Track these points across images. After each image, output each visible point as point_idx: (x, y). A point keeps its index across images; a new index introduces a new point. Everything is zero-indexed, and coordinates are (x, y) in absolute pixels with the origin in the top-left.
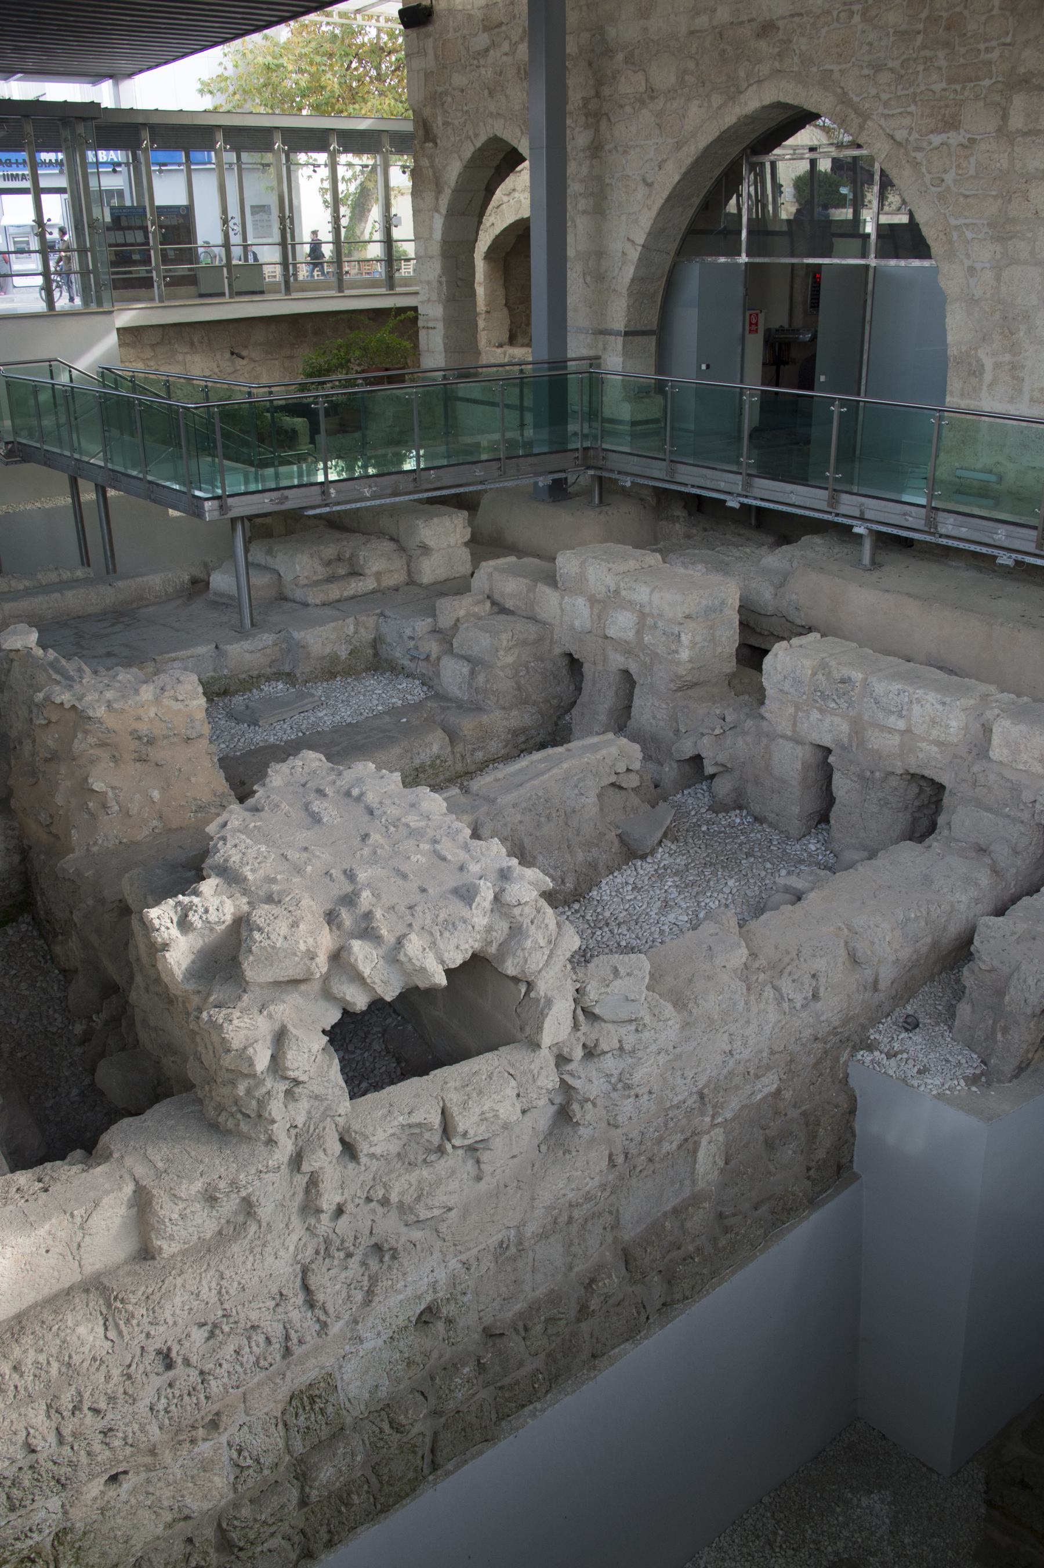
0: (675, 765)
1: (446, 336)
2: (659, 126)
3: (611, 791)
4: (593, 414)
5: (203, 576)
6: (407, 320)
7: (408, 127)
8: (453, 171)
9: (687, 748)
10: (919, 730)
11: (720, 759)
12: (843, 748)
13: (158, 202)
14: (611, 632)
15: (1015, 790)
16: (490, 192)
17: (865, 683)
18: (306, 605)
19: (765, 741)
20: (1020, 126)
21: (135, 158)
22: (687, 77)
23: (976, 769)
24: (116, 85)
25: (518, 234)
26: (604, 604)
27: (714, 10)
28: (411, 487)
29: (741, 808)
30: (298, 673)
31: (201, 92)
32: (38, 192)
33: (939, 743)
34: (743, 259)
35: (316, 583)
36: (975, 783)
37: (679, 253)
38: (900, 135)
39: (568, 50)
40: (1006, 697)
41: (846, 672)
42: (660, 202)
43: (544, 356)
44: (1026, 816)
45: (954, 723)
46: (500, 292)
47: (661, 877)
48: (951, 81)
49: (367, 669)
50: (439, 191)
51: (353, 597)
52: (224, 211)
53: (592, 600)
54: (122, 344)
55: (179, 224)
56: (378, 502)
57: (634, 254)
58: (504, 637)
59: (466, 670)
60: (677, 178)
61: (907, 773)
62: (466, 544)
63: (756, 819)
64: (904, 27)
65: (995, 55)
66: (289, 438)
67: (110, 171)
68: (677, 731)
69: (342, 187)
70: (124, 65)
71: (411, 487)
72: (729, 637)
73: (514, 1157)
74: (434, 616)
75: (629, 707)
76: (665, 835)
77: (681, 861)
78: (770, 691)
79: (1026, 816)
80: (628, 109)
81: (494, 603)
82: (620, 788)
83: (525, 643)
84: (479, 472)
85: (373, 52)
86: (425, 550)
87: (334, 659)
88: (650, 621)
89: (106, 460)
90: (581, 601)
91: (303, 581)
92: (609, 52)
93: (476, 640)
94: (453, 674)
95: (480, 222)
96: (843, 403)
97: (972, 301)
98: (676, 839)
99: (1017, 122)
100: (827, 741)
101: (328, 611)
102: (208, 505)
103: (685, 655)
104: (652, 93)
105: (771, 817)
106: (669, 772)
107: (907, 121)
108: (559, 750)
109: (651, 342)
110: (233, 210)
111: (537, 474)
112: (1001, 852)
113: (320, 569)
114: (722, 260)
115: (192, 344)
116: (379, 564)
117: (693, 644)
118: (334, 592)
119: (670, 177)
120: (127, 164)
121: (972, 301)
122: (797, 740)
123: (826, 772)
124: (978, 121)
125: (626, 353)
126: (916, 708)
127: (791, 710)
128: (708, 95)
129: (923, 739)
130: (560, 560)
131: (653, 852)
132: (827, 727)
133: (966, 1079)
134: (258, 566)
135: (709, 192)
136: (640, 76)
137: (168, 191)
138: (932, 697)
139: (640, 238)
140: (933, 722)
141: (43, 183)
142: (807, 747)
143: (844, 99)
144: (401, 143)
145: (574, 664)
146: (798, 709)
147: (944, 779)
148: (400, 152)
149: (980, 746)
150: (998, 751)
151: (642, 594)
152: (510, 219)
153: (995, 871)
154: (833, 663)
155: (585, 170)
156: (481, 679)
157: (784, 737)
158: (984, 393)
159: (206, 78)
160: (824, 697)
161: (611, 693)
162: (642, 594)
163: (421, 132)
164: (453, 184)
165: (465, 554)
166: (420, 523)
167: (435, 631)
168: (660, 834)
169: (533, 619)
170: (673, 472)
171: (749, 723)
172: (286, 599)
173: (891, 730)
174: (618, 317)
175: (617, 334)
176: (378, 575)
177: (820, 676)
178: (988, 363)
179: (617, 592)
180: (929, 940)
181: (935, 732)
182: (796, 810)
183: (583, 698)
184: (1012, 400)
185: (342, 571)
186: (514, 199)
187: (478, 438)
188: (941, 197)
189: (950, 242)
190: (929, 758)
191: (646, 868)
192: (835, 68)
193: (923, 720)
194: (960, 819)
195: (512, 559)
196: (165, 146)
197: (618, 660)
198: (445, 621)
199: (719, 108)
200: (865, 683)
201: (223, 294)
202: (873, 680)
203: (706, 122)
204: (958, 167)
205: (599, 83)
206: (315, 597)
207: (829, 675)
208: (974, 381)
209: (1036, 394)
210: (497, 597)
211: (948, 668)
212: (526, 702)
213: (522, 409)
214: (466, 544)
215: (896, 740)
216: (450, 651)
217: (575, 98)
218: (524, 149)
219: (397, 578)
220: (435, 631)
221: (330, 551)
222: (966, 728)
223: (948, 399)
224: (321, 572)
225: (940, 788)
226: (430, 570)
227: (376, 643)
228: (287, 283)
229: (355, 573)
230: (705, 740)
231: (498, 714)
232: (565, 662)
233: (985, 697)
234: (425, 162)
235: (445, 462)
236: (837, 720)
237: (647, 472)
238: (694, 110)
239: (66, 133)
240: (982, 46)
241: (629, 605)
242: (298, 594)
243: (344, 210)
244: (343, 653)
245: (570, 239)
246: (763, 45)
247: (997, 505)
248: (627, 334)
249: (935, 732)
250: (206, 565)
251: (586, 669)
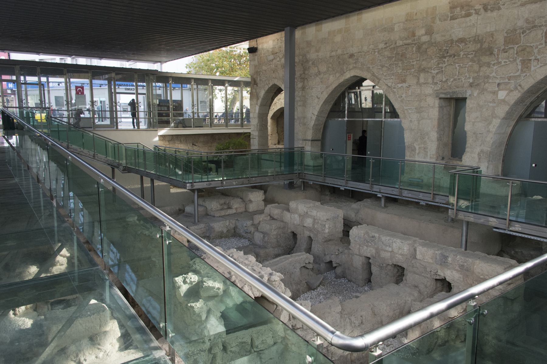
0: (324, 264)
1: (259, 141)
2: (322, 82)
3: (304, 269)
4: (302, 164)
5: (182, 208)
6: (247, 136)
7: (249, 80)
8: (262, 93)
9: (328, 259)
10: (396, 251)
11: (337, 261)
12: (374, 257)
13: (173, 99)
14: (305, 225)
15: (425, 268)
16: (273, 99)
17: (379, 238)
18: (214, 217)
19: (351, 256)
20: (423, 81)
21: (166, 85)
23: (413, 262)
24: (161, 64)
25: (281, 112)
26: (303, 216)
27: (337, 51)
28: (247, 182)
29: (344, 278)
30: (211, 236)
31: (187, 67)
32: (137, 94)
33: (401, 255)
34: (346, 119)
35: (218, 210)
36: (413, 267)
37: (327, 118)
38: (389, 84)
39: (296, 61)
40: (421, 241)
41: (373, 234)
42: (322, 103)
43: (288, 146)
44: (429, 276)
45: (405, 248)
46: (276, 129)
47: (319, 296)
49: (232, 236)
50: (258, 99)
51: (228, 215)
52: (193, 102)
53: (300, 216)
54: (160, 140)
55: (179, 105)
56: (237, 186)
57: (314, 118)
58: (273, 226)
59: (262, 236)
60: (327, 96)
61: (393, 264)
62: (263, 200)
63: (349, 281)
66: (211, 170)
67: (159, 89)
68: (325, 255)
69: (228, 96)
70: (164, 59)
71: (247, 182)
72: (340, 227)
73: (271, 359)
74: (253, 220)
75: (310, 248)
76: (320, 284)
77: (325, 291)
78: (352, 241)
79: (429, 276)
80: (313, 77)
81: (271, 217)
82: (307, 268)
83: (280, 228)
84: (267, 179)
85: (238, 57)
86: (251, 201)
87: (222, 232)
88: (317, 221)
89: (156, 171)
90: (296, 216)
91: (213, 210)
92: (307, 61)
93: (265, 227)
94: (258, 237)
95: (270, 108)
96: (373, 159)
98: (324, 285)
99: (422, 80)
100: (369, 256)
101: (221, 219)
102: (188, 185)
103: (327, 231)
104: (319, 73)
105: (353, 280)
106: (323, 266)
107: (391, 81)
108: (289, 256)
109: (319, 143)
110: (195, 103)
111: (285, 180)
112: (422, 287)
113: (219, 206)
114: (340, 119)
115: (181, 141)
116: (237, 205)
117: (329, 228)
118: (223, 213)
119: (325, 96)
120: (163, 87)
121: (412, 130)
122: (360, 255)
123: (370, 264)
124: (411, 81)
125: (312, 146)
126: (394, 244)
127: (358, 246)
128: (335, 74)
129: (397, 254)
130: (291, 204)
131: (316, 288)
132: (369, 251)
133: (412, 353)
134: (200, 205)
135: (336, 100)
136: (316, 68)
137: (176, 95)
138: (398, 241)
139: (316, 113)
140: (400, 248)
141: (139, 92)
142: (364, 258)
143: (373, 75)
144: (247, 84)
145: (294, 235)
146: (360, 246)
147: (404, 266)
148: (246, 86)
149: (414, 256)
150: (419, 256)
151: (314, 213)
152: (279, 107)
153: (420, 292)
154: (370, 232)
155: (300, 94)
156: (266, 238)
157: (357, 255)
158: (416, 156)
159: (188, 63)
160: (368, 242)
161: (305, 244)
162: (314, 213)
163: (253, 82)
164: (262, 97)
165: (263, 203)
166: (250, 193)
167: (253, 225)
168: (318, 283)
169: (283, 221)
170: (325, 179)
171: (346, 251)
172: (208, 215)
173: (387, 251)
174: (309, 136)
175: (309, 140)
176: (236, 209)
177: (366, 236)
178: (417, 147)
179: (307, 213)
180: (399, 311)
181: (400, 251)
182: (361, 277)
183: (297, 245)
184: (424, 158)
185: (225, 207)
186: (280, 102)
187: (267, 170)
188: (402, 101)
189: (404, 113)
190: (399, 259)
191: (314, 293)
193: (396, 248)
194: (409, 277)
195: (277, 204)
196: (176, 83)
197: (307, 233)
198: (256, 222)
200: (379, 238)
201: (191, 127)
202: (381, 236)
203: (334, 81)
204: (406, 93)
205: (305, 69)
206: (217, 214)
207: (368, 236)
208: (413, 152)
209: (432, 156)
210: (272, 215)
211: (405, 234)
212: (280, 246)
213: (280, 162)
214: (263, 200)
215: (389, 254)
216: (257, 230)
217: (298, 74)
218: (283, 87)
219: (243, 210)
220: (253, 225)
221: (222, 201)
222: (409, 250)
223: (406, 158)
224: (220, 207)
225: (403, 269)
226: (252, 207)
227: (235, 228)
228: (211, 124)
229: (230, 208)
230: (333, 256)
231: (271, 249)
232: (292, 234)
233: (415, 241)
234: (254, 91)
235: (256, 176)
236: (371, 249)
237: (317, 180)
238: (332, 78)
239: (146, 78)
241: (311, 216)
242: (212, 213)
243: (228, 103)
244: (225, 231)
245: (296, 113)
246: (351, 60)
247: (422, 188)
248: (312, 140)
249: (400, 251)
250: (183, 205)
251: (298, 236)
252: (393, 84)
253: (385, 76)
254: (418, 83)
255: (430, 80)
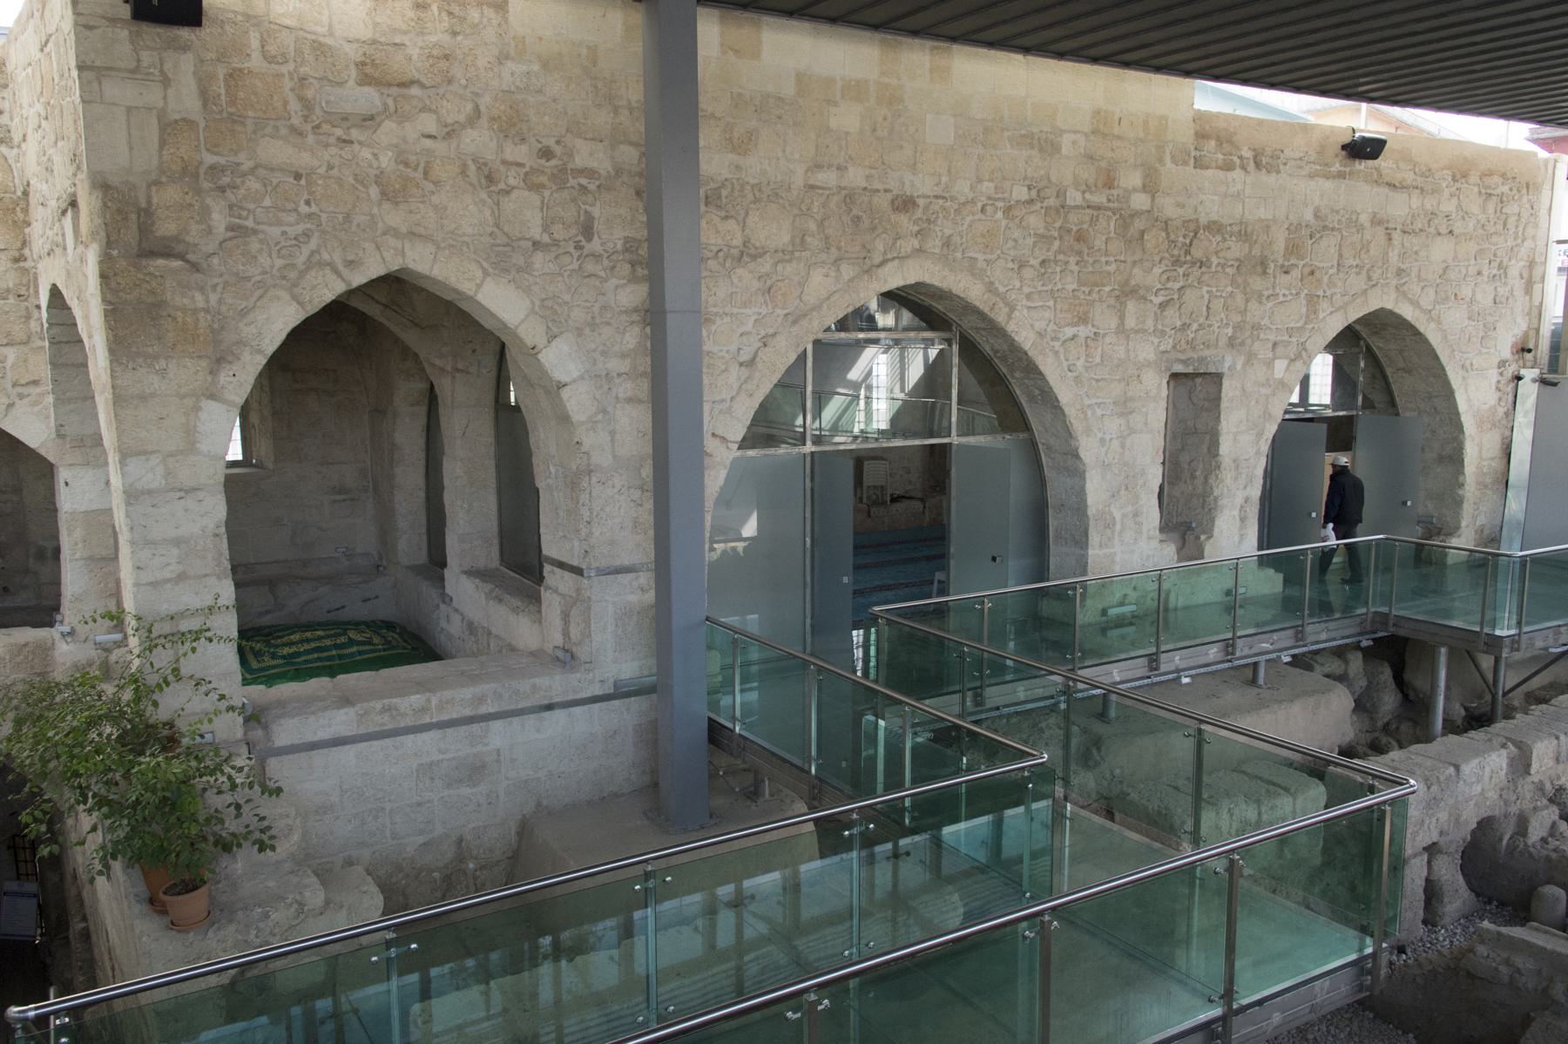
22: (809, 239)
48: (1081, 283)
64: (1041, 231)
65: (1112, 268)
97: (1106, 467)
99: (1130, 322)
107: (1048, 314)
121: (1106, 467)
178: (1118, 515)
192: (980, 257)
199: (852, 280)
208: (1109, 532)
240: (1103, 259)
252: (1052, 326)
253: (1028, 296)
254: (1121, 330)
255: (1150, 323)
